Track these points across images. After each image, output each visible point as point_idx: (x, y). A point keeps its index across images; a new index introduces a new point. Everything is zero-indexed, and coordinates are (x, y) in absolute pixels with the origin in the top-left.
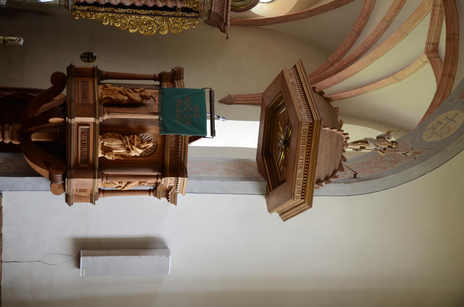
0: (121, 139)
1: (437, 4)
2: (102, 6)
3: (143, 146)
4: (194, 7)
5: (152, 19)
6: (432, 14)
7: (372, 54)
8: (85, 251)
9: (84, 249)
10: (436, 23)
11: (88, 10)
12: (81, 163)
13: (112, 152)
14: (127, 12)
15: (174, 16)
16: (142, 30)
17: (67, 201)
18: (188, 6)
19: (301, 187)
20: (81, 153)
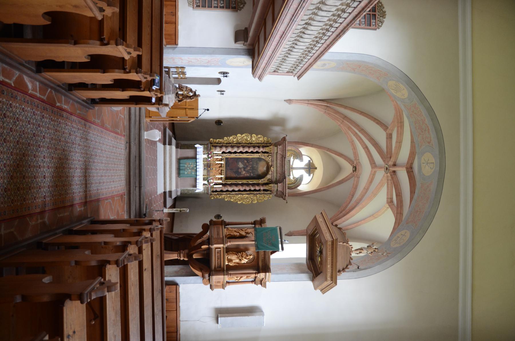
0: (236, 255)
2: (224, 192)
3: (248, 258)
4: (269, 189)
5: (249, 196)
8: (221, 315)
9: (220, 313)
10: (390, 188)
11: (218, 194)
12: (218, 268)
13: (232, 261)
14: (236, 194)
15: (260, 194)
16: (244, 202)
17: (211, 288)
19: (330, 274)
20: (217, 263)
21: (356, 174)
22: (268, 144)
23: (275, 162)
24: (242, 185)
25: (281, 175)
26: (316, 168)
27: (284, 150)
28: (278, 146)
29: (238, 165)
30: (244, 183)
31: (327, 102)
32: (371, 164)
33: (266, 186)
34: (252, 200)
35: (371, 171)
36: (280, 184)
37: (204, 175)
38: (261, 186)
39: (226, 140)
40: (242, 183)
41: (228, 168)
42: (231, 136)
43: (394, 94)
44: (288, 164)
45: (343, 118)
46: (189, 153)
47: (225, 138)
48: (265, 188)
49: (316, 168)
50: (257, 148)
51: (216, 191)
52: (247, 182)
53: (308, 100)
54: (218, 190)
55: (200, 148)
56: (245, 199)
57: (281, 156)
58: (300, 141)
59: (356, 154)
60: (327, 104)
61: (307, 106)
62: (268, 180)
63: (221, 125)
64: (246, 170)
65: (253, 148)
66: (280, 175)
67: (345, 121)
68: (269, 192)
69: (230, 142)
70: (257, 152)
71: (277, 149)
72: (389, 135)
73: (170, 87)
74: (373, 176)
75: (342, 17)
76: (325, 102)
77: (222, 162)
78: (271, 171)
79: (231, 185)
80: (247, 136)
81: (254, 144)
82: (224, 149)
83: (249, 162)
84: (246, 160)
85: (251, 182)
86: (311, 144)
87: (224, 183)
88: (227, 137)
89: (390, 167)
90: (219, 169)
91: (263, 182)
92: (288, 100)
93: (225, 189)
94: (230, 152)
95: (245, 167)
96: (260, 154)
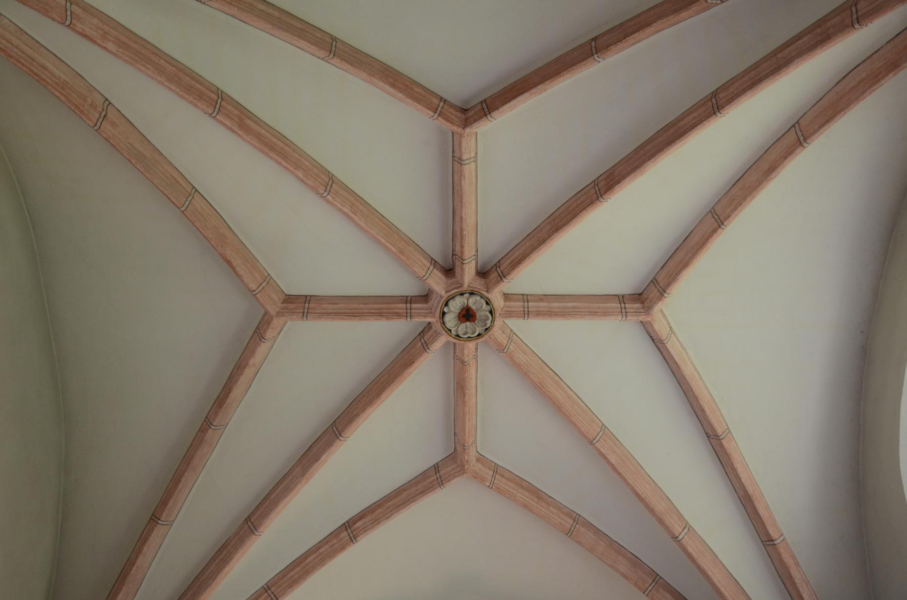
1: (523, 309)
6: (547, 314)
7: (673, 522)
10: (570, 305)
35: (476, 477)
74: (502, 476)
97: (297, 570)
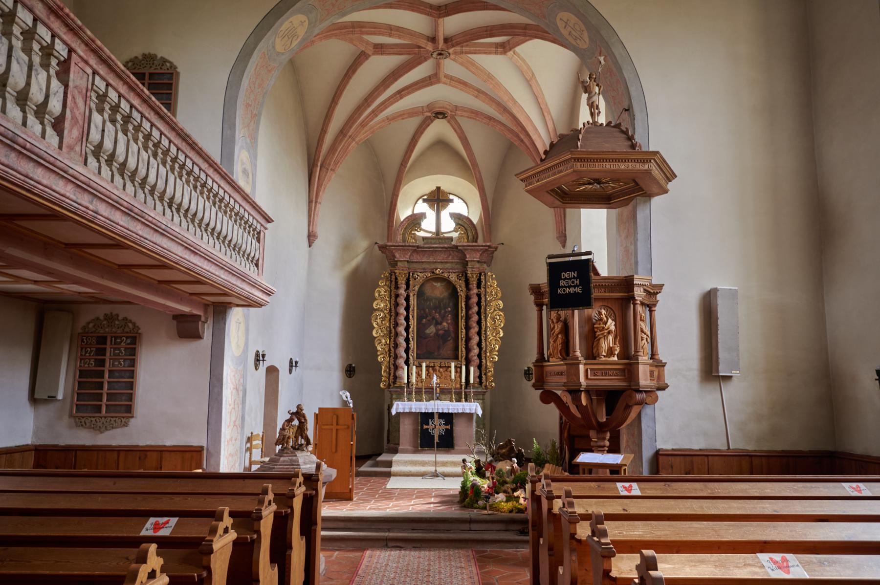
0: (599, 340)
2: (481, 362)
3: (605, 318)
8: (714, 371)
9: (711, 372)
12: (625, 376)
13: (611, 348)
15: (485, 295)
16: (500, 325)
17: (664, 389)
18: (475, 282)
19: (638, 164)
20: (615, 376)
21: (449, 112)
22: (391, 278)
23: (427, 266)
24: (468, 328)
25: (450, 254)
26: (438, 188)
27: (404, 248)
28: (396, 259)
29: (431, 335)
30: (465, 324)
31: (313, 167)
32: (431, 84)
33: (471, 282)
34: (496, 309)
36: (468, 256)
37: (451, 401)
38: (472, 292)
39: (383, 358)
40: (465, 328)
41: (436, 353)
42: (376, 347)
43: (299, 40)
44: (430, 241)
45: (345, 136)
46: (406, 430)
47: (379, 360)
48: (475, 285)
49: (438, 188)
50: (398, 299)
51: (480, 377)
52: (464, 318)
53: (310, 202)
54: (478, 374)
55: (399, 407)
56: (495, 323)
57: (415, 255)
58: (386, 219)
59: (411, 113)
60: (317, 165)
61: (320, 203)
62: (460, 280)
63: (354, 367)
64: (440, 320)
65: (398, 308)
66: (451, 257)
67: (350, 134)
68: (482, 277)
69: (387, 350)
70: (407, 299)
71: (401, 261)
72: (377, 50)
73: (284, 461)
74: (453, 80)
75: (176, 155)
76: (314, 170)
77: (424, 365)
78: (443, 273)
79: (468, 350)
80: (377, 319)
81: (392, 305)
82: (401, 362)
83: (425, 315)
84: (422, 320)
85: (464, 312)
86: (392, 198)
87: (464, 362)
88: (378, 355)
89: (438, 48)
90: (439, 371)
91: (463, 288)
92: (309, 240)
93: (476, 360)
94: (407, 351)
95: (434, 321)
96: (411, 295)
97: (382, 106)
